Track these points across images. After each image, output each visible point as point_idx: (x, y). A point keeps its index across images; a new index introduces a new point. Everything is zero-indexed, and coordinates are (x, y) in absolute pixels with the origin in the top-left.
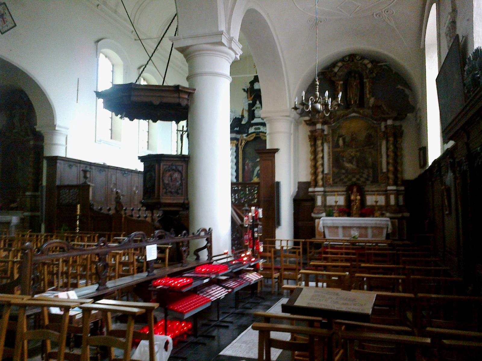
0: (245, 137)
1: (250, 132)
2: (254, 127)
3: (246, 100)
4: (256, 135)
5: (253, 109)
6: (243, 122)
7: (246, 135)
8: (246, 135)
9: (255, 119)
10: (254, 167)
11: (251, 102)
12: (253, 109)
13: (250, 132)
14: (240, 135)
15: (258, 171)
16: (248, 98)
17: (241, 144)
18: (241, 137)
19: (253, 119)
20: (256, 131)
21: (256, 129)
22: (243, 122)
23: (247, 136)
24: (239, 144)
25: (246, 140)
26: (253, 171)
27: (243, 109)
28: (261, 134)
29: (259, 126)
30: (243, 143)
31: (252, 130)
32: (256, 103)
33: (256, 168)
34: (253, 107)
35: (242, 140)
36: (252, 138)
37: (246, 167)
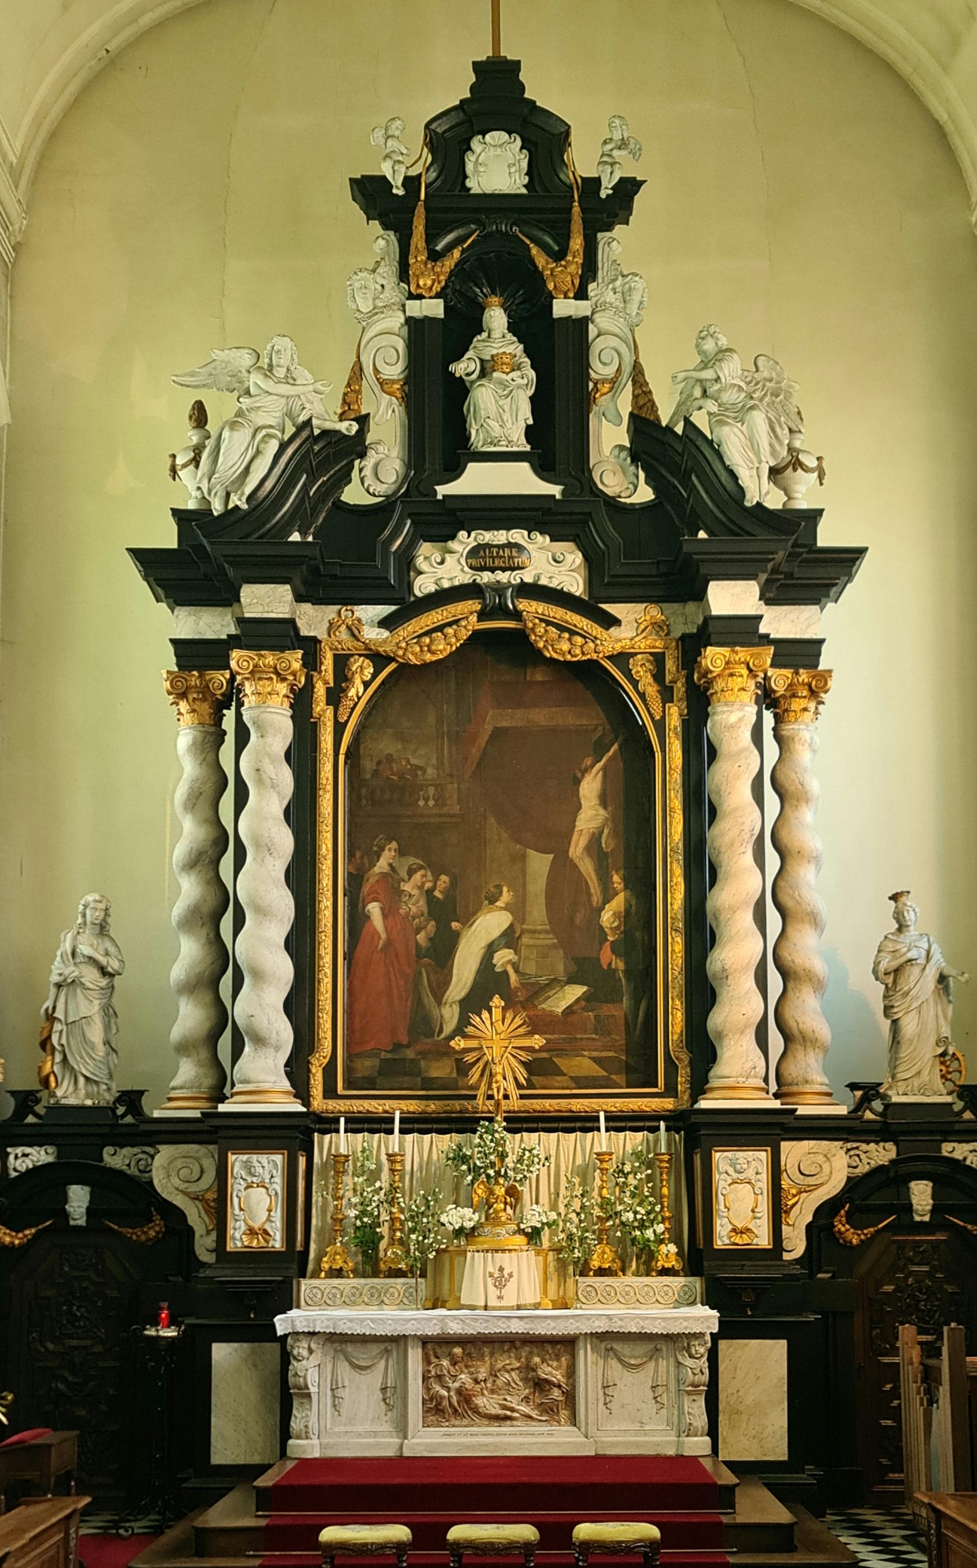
0: (373, 634)
1: (423, 586)
2: (464, 542)
3: (393, 293)
4: (482, 616)
5: (459, 368)
6: (353, 495)
7: (385, 610)
8: (385, 610)
9: (472, 466)
10: (448, 915)
11: (434, 308)
12: (459, 368)
13: (423, 586)
14: (330, 611)
15: (491, 949)
16: (404, 274)
17: (335, 696)
18: (332, 628)
19: (454, 471)
20: (486, 578)
21: (480, 557)
22: (353, 495)
23: (386, 623)
24: (320, 690)
25: (379, 659)
26: (443, 950)
27: (358, 372)
28: (529, 607)
29: (518, 536)
30: (356, 689)
31: (441, 566)
32: (478, 328)
33: (468, 919)
34: (458, 357)
35: (342, 662)
36: (443, 647)
37: (374, 909)
